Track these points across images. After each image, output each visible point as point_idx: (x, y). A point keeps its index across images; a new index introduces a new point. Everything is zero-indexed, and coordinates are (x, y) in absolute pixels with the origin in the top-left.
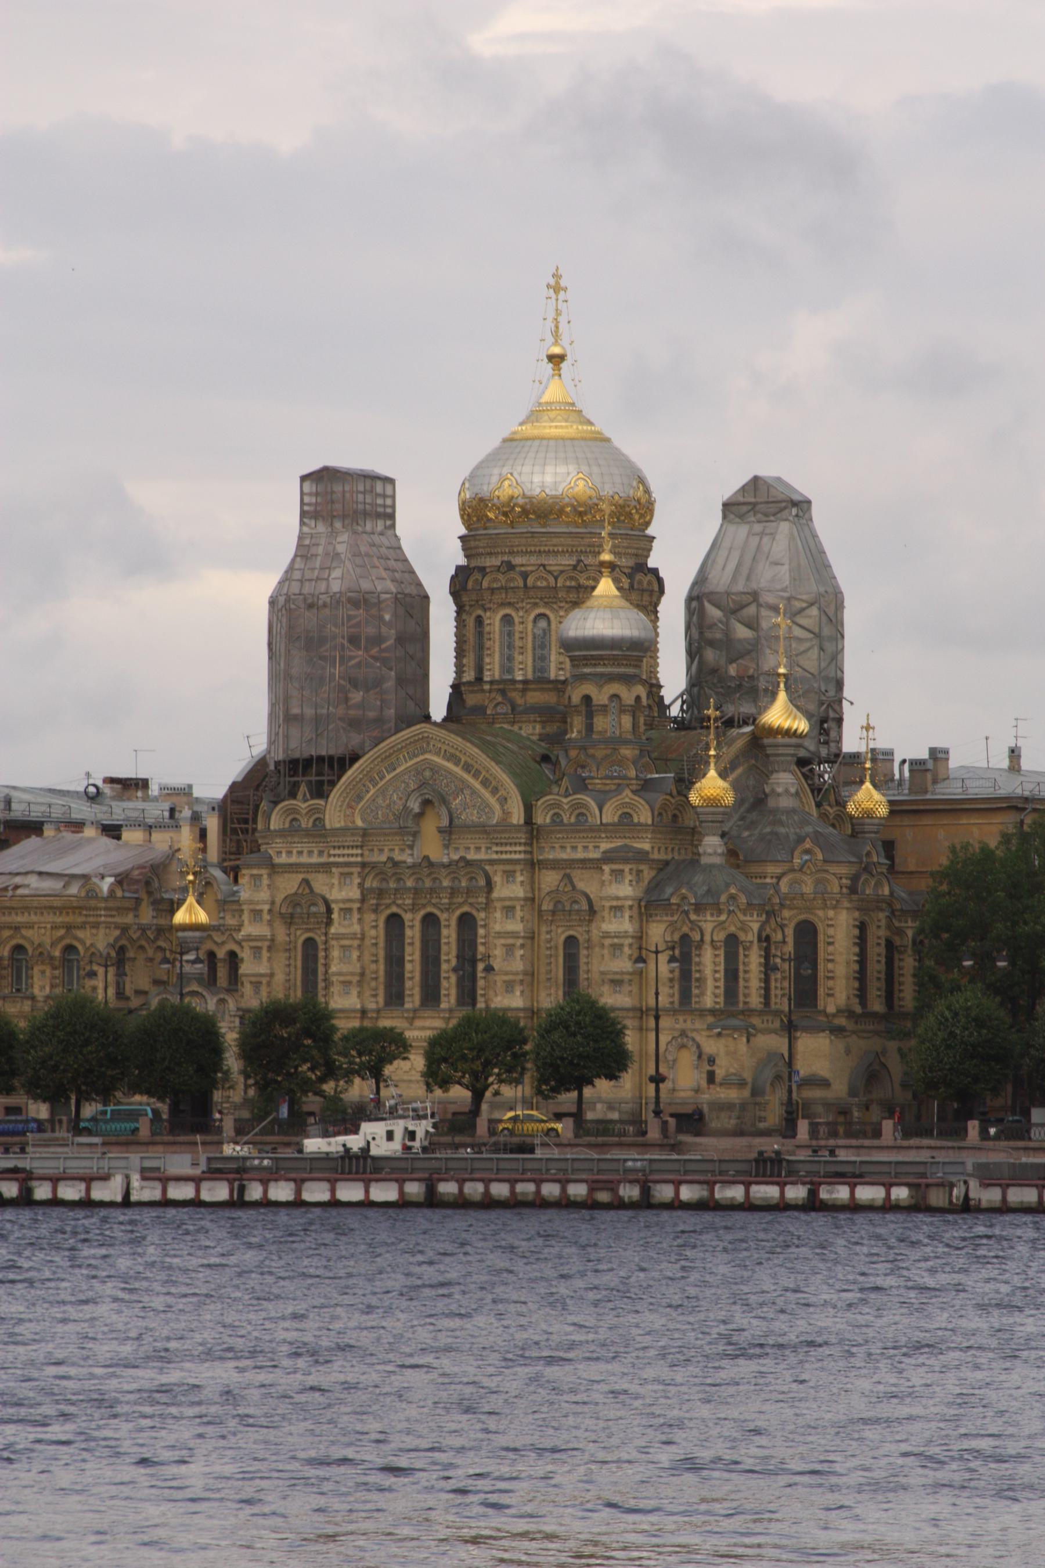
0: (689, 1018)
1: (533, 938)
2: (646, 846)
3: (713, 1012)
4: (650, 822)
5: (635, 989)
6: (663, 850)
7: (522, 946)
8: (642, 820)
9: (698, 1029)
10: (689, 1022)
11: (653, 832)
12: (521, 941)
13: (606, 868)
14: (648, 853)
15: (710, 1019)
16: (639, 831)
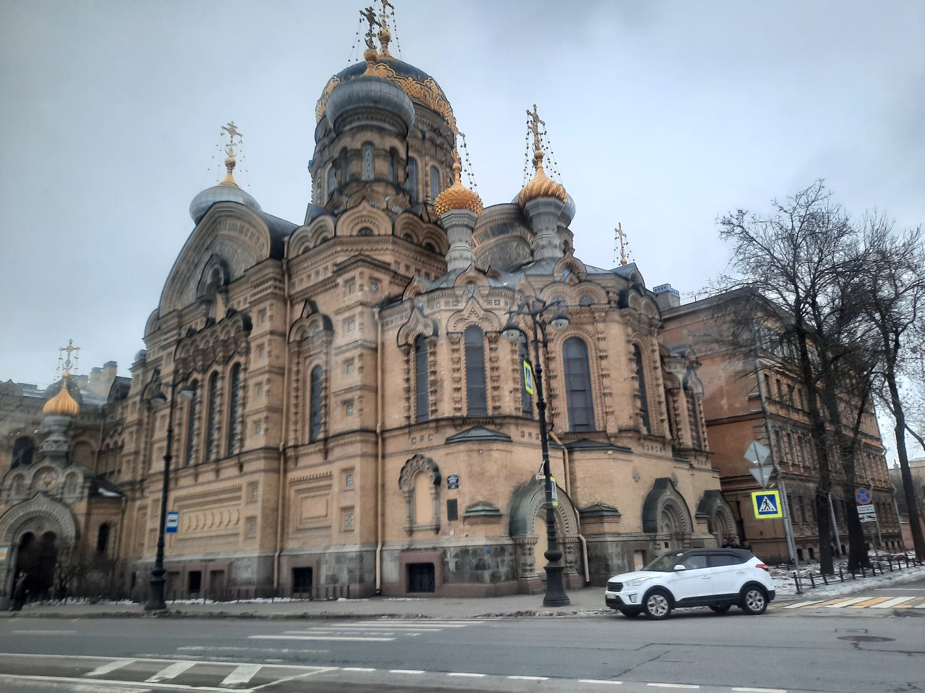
0: (425, 433)
1: (283, 374)
2: (388, 258)
3: (453, 421)
4: (390, 232)
5: (369, 409)
6: (413, 269)
7: (269, 381)
8: (382, 232)
9: (431, 442)
10: (426, 439)
11: (394, 243)
12: (266, 376)
13: (340, 281)
14: (389, 264)
15: (450, 432)
16: (377, 242)
